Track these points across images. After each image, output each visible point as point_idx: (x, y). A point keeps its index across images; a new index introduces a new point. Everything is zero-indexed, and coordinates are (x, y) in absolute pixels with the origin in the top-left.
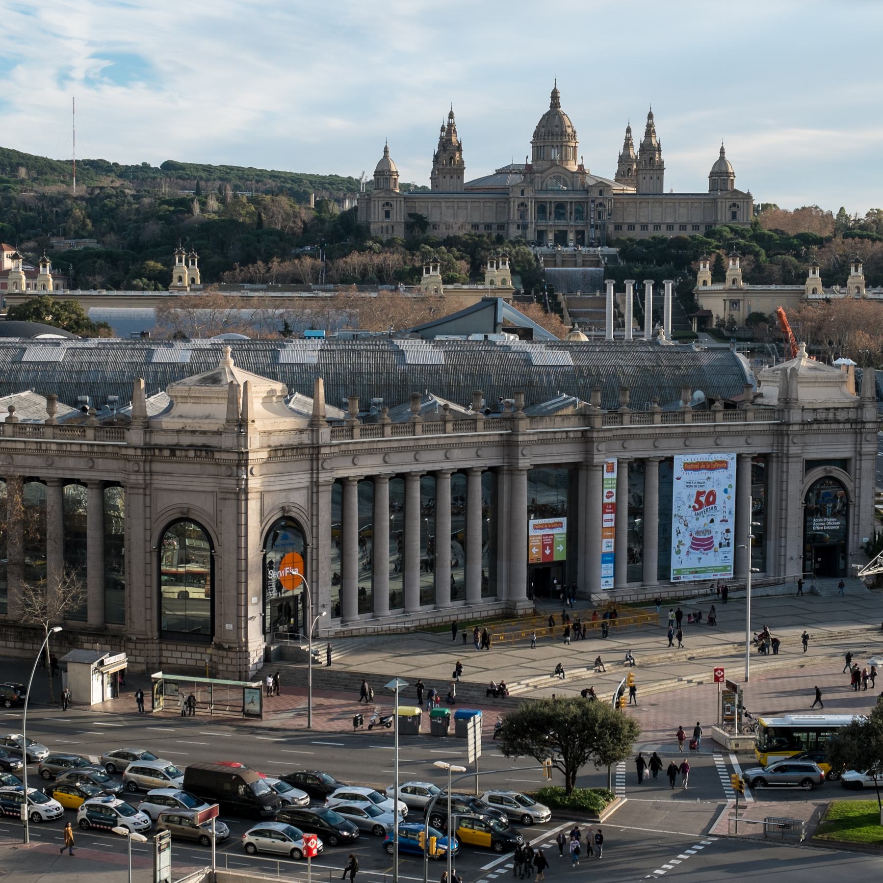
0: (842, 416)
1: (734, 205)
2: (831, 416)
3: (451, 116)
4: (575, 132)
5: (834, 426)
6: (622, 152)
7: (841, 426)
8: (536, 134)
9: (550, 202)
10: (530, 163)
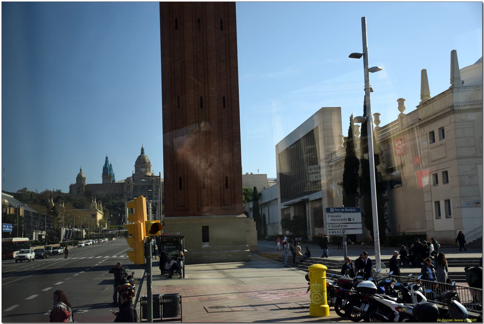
4: (150, 162)
8: (136, 162)
9: (139, 186)
10: (134, 173)
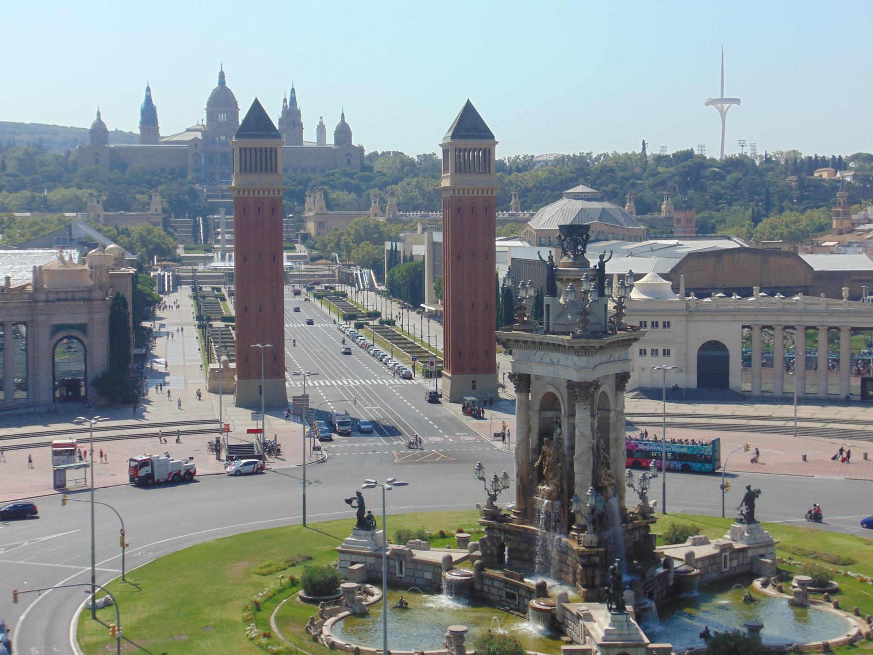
0: (77, 296)
1: (348, 154)
2: (70, 296)
3: (148, 89)
5: (71, 303)
6: (280, 116)
7: (77, 303)
